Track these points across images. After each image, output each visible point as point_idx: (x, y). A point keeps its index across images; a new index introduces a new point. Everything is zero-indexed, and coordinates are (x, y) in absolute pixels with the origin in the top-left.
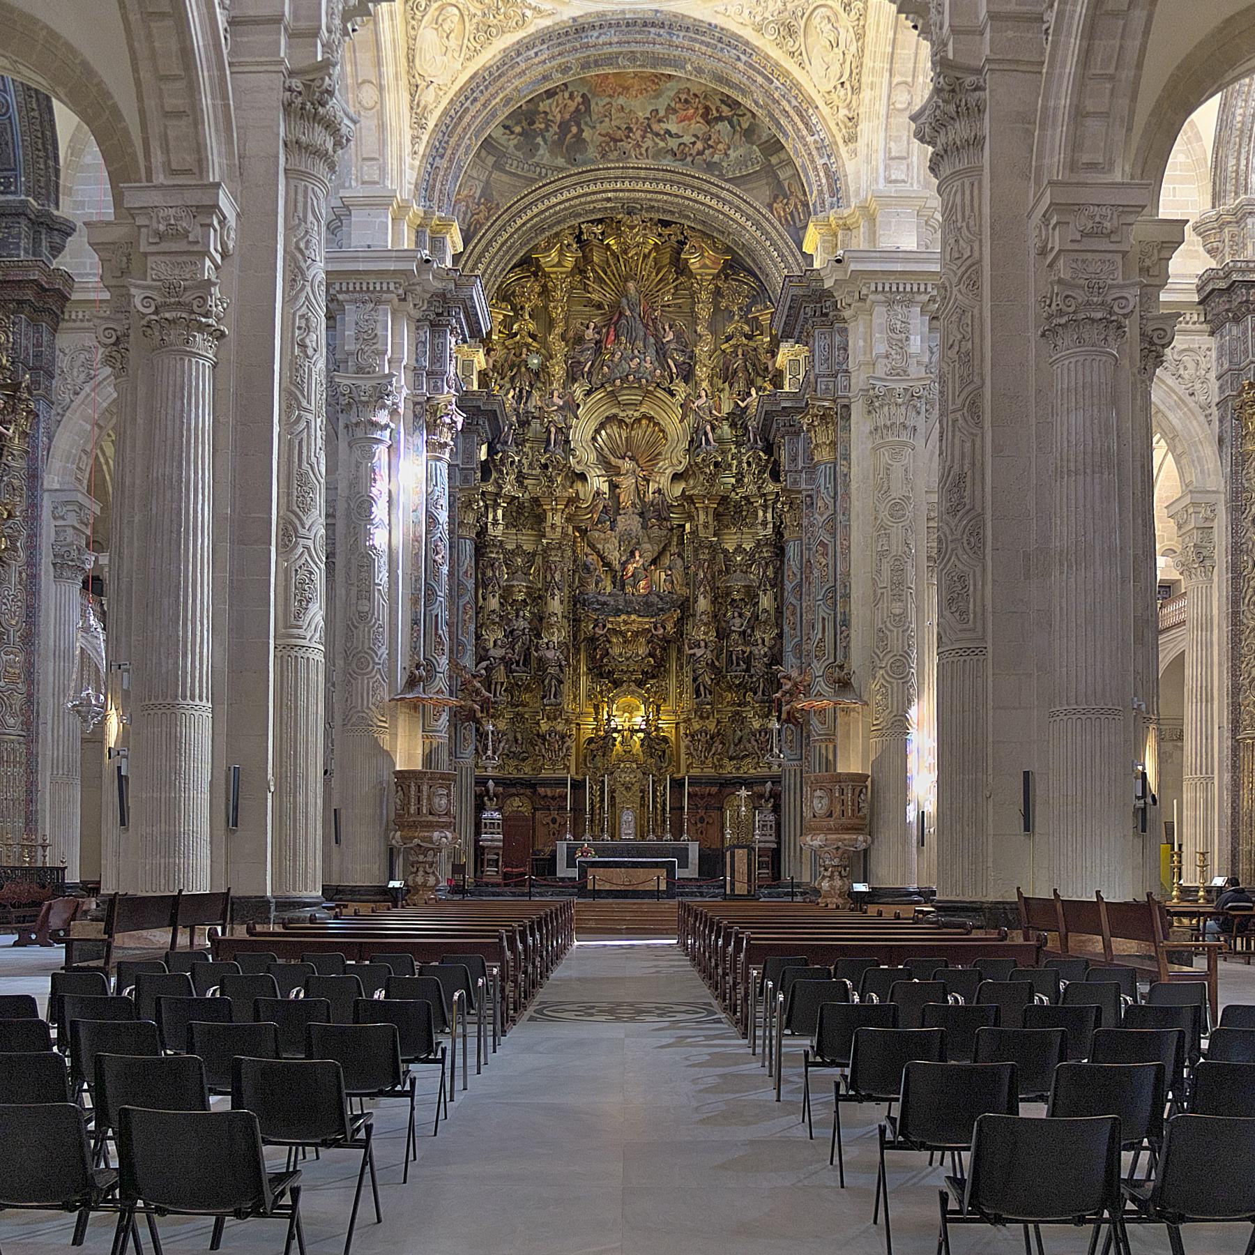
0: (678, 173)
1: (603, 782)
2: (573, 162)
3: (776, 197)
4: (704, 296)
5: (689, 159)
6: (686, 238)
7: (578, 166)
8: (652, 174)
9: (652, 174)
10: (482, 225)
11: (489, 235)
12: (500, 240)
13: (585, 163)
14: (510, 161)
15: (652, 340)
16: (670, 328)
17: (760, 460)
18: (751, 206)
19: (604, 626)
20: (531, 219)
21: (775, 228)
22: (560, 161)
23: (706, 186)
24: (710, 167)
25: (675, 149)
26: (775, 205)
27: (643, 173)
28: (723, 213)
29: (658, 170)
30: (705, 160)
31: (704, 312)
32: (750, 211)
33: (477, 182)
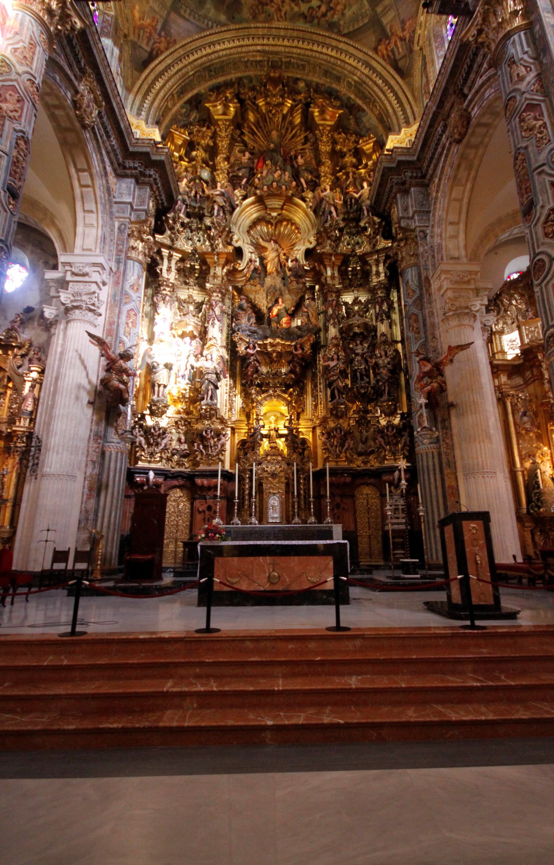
0: (308, 32)
1: (251, 471)
2: (232, 19)
3: (379, 42)
4: (324, 139)
5: (316, 21)
6: (312, 99)
7: (236, 23)
8: (289, 33)
9: (289, 33)
10: (162, 53)
11: (169, 61)
12: (177, 68)
13: (241, 22)
14: (184, 7)
15: (289, 168)
16: (302, 157)
17: (374, 223)
18: (361, 51)
19: (254, 348)
20: (201, 58)
21: (379, 63)
22: (223, 18)
23: (328, 41)
24: (332, 26)
25: (306, 12)
26: (380, 47)
27: (282, 33)
28: (340, 60)
29: (293, 30)
30: (327, 21)
31: (325, 148)
32: (361, 55)
33: (158, 17)
